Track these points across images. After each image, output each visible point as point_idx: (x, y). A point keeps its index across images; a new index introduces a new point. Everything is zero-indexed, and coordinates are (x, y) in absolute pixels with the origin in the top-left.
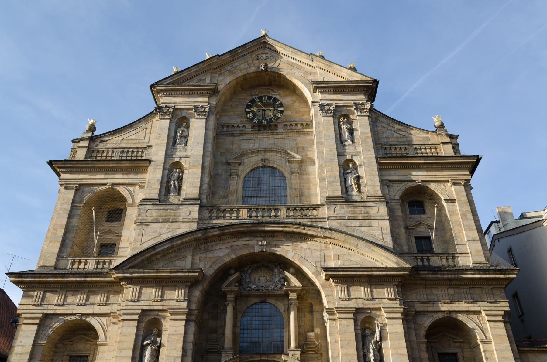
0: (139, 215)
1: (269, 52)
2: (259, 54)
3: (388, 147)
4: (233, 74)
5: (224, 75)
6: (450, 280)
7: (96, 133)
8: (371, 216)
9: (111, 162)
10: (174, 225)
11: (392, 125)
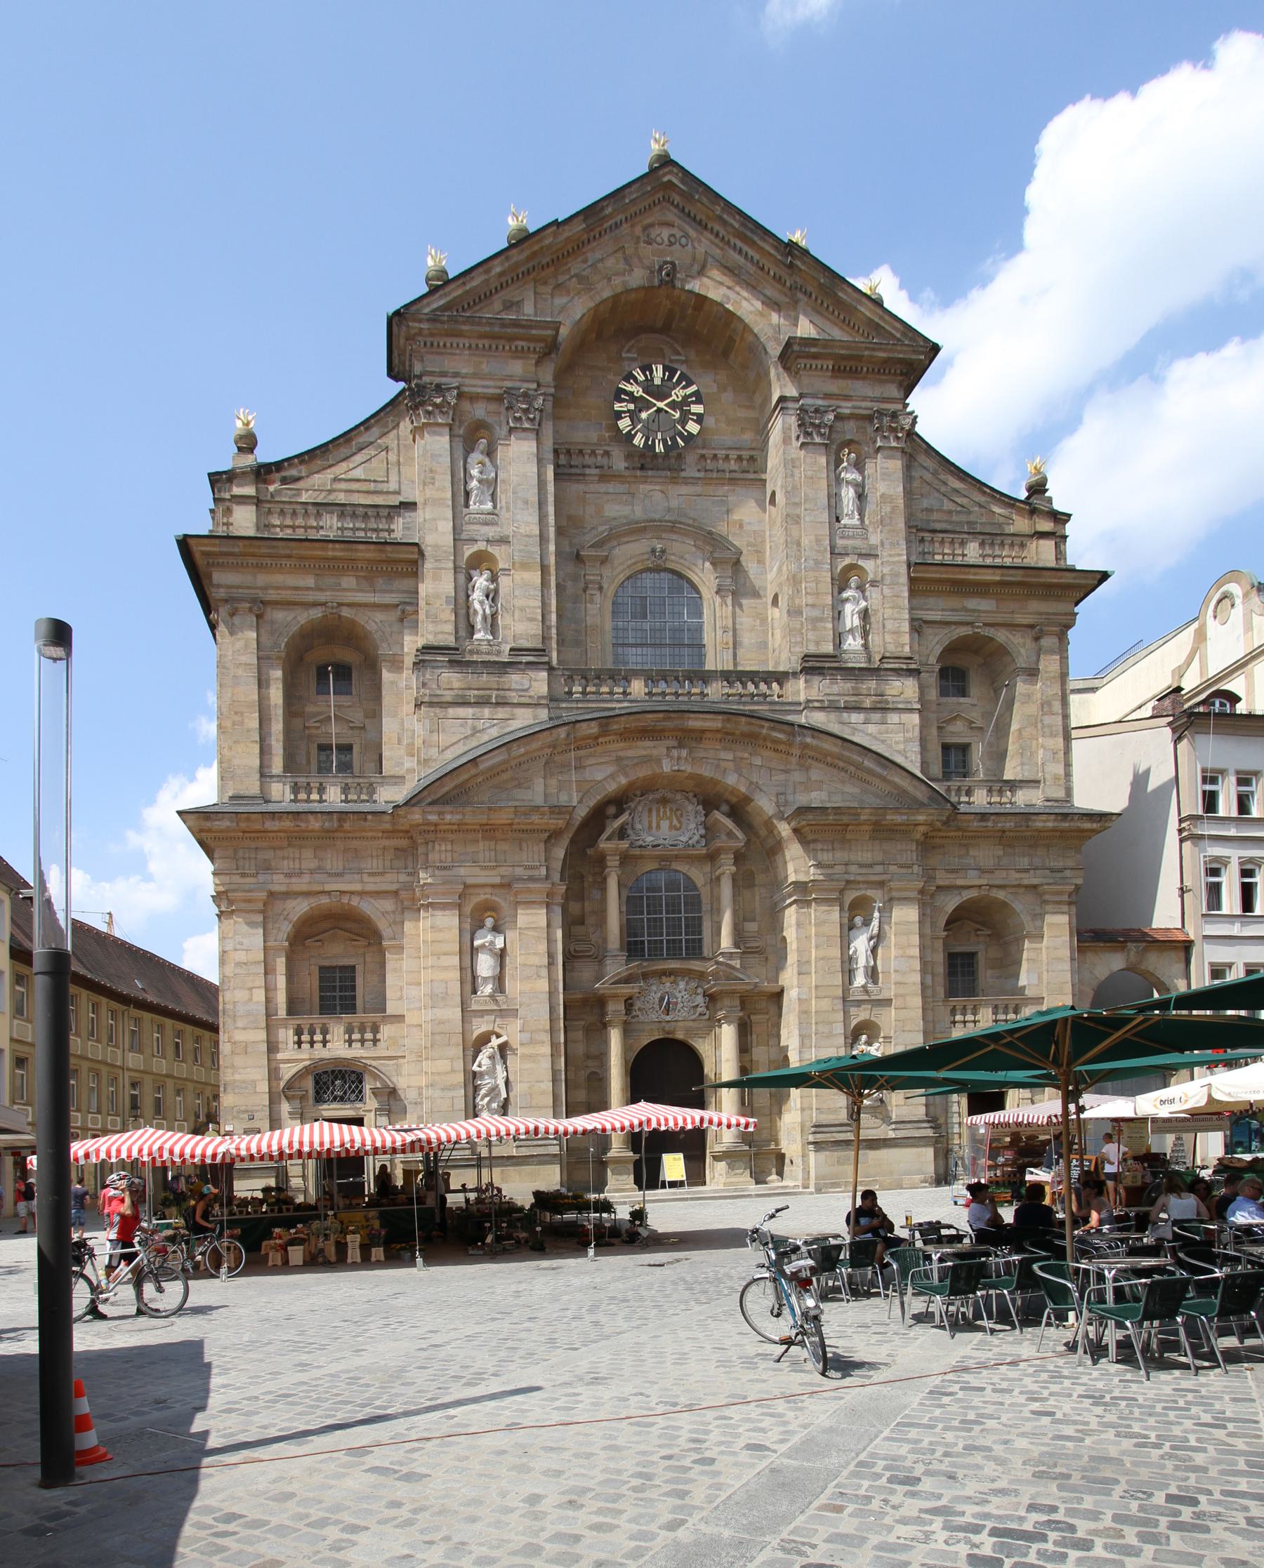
1: (678, 222)
2: (652, 225)
3: (927, 536)
4: (590, 290)
5: (568, 293)
7: (266, 453)
8: (888, 703)
9: (330, 546)
10: (502, 713)
11: (942, 477)
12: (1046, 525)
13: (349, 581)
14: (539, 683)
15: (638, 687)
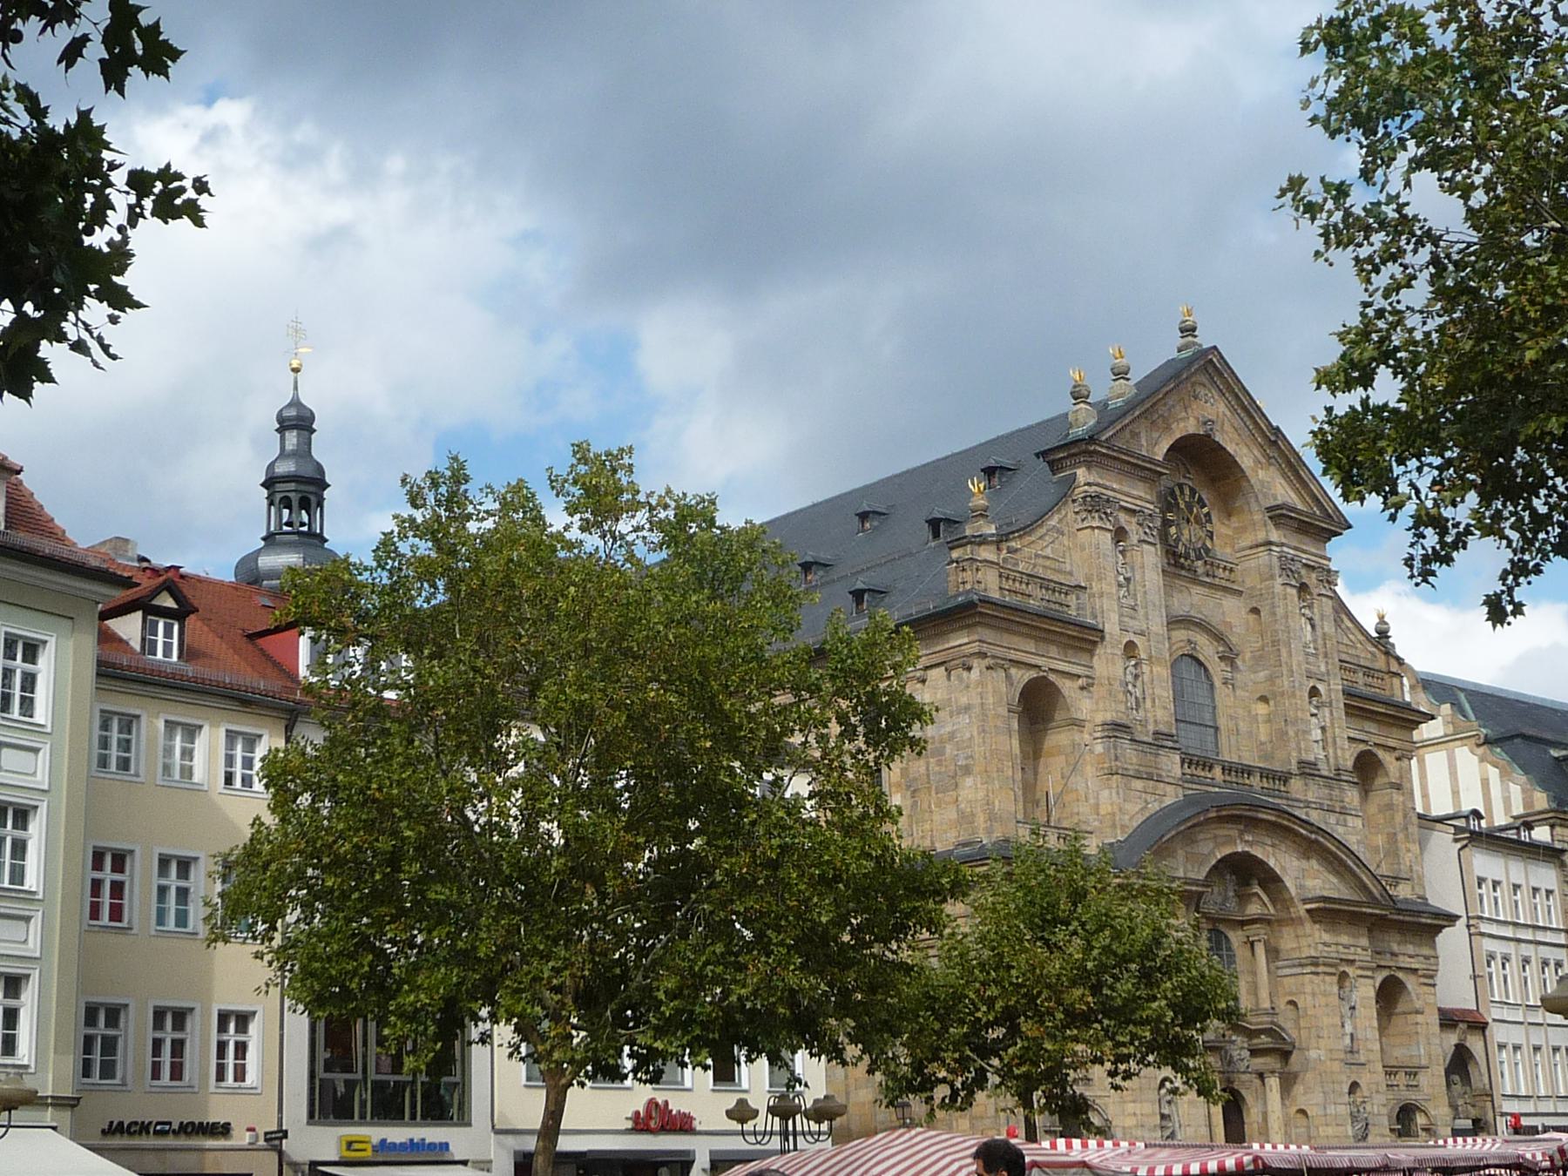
13: (1053, 651)
14: (1171, 764)
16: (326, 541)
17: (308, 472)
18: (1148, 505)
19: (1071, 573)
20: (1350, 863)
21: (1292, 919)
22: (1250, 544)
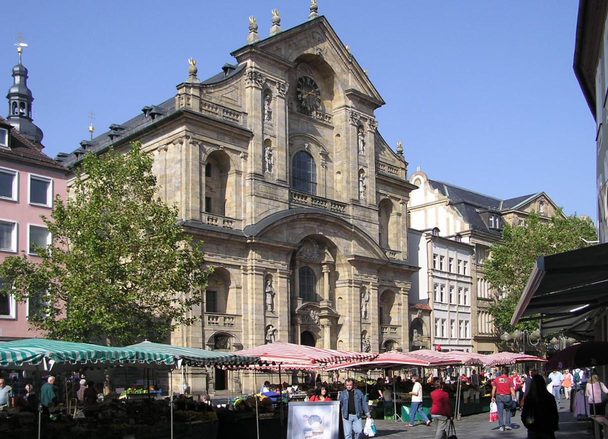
0: (255, 188)
6: (395, 269)
10: (276, 204)
12: (403, 166)
15: (309, 200)
16: (33, 120)
17: (24, 92)
18: (282, 81)
19: (241, 107)
20: (369, 242)
21: (342, 264)
22: (337, 106)
